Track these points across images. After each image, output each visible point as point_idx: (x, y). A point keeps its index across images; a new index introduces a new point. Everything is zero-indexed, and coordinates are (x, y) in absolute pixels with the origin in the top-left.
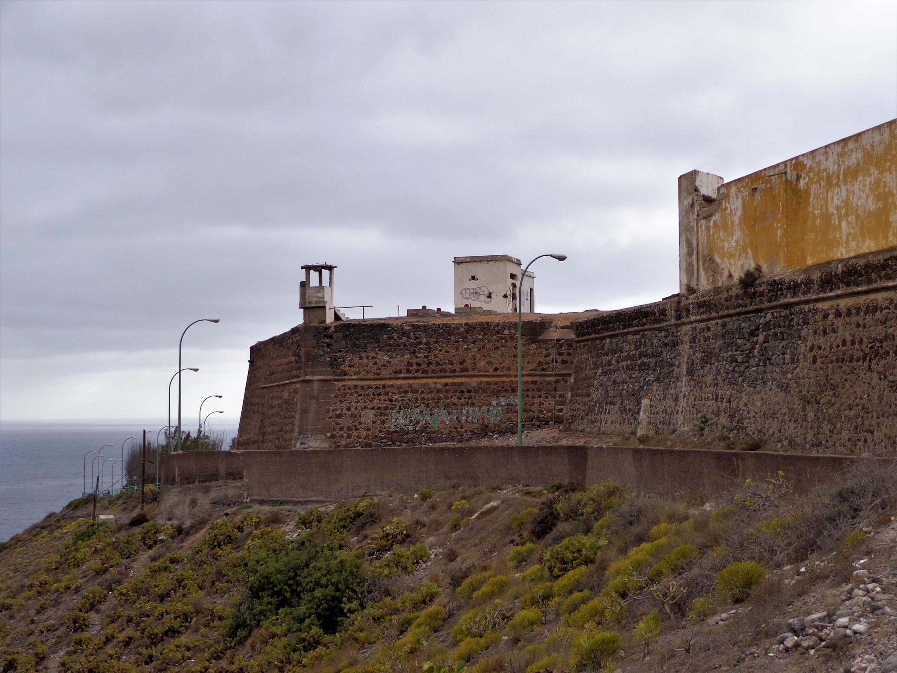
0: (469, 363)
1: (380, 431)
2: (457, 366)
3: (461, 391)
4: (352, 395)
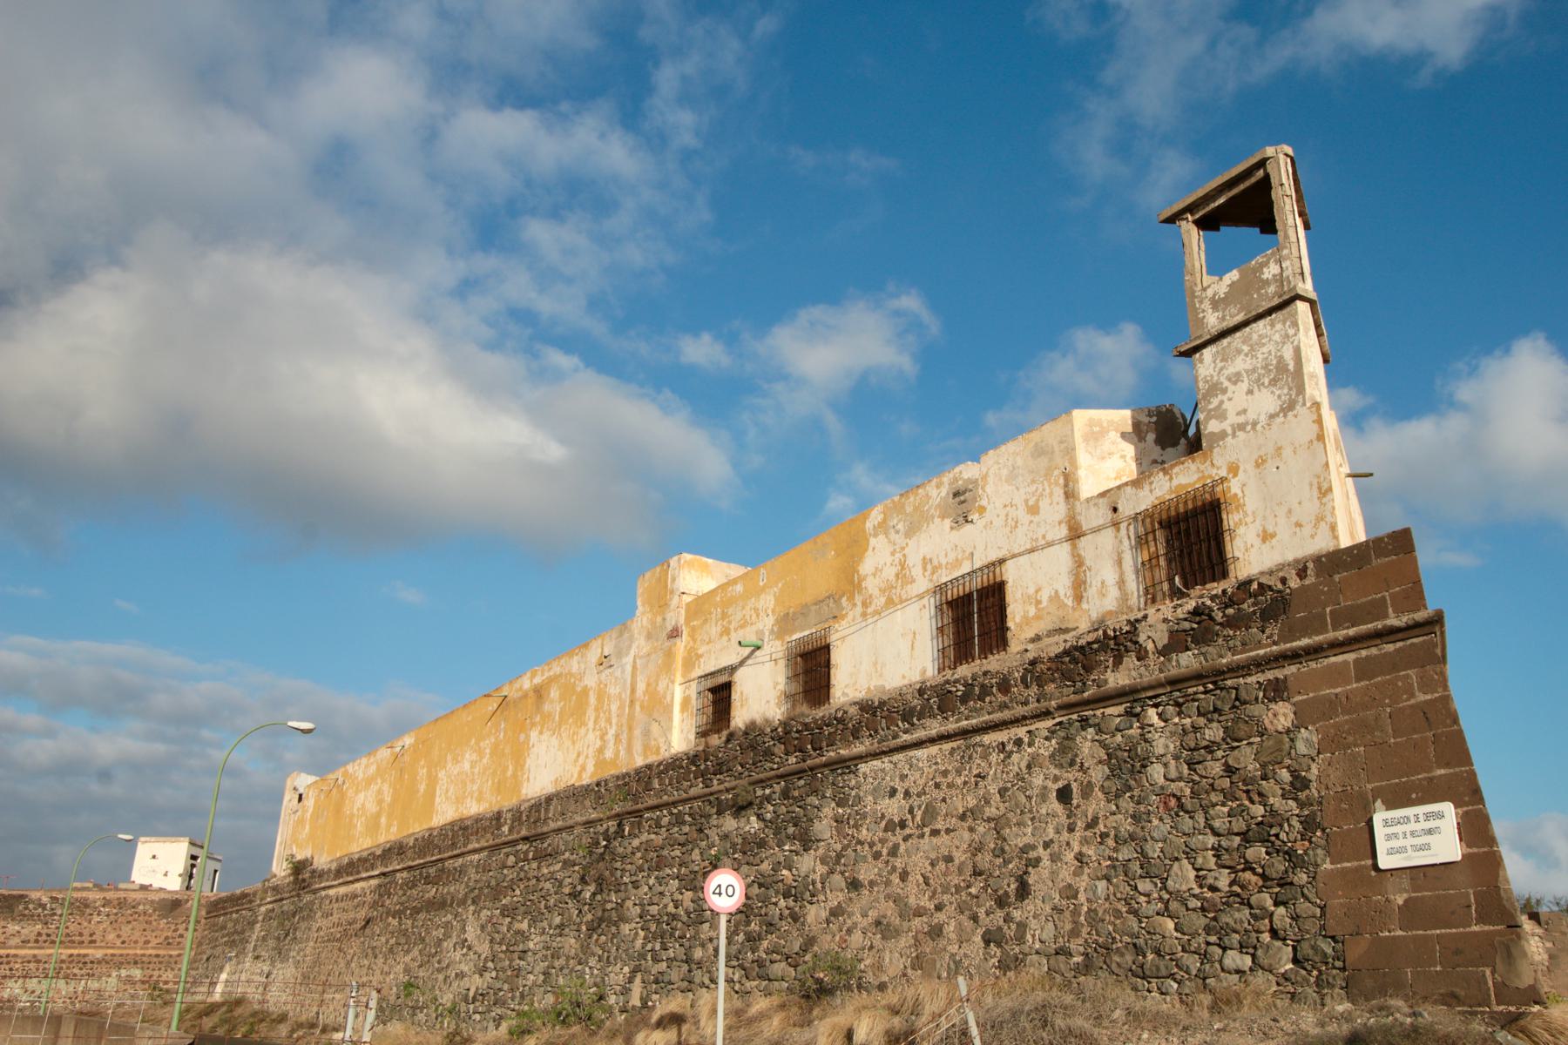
0: (99, 934)
2: (86, 938)
3: (83, 961)
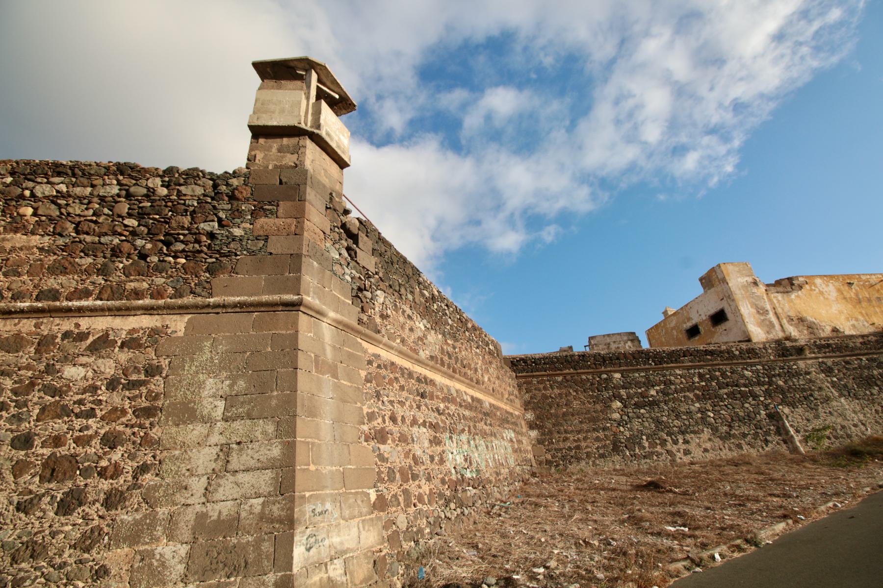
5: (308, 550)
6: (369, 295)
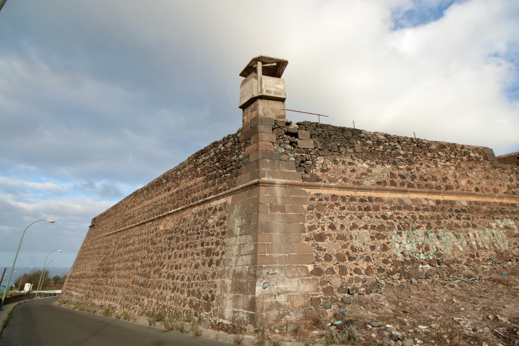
0: (451, 181)
1: (385, 262)
4: (331, 207)
5: (264, 288)
6: (310, 162)
